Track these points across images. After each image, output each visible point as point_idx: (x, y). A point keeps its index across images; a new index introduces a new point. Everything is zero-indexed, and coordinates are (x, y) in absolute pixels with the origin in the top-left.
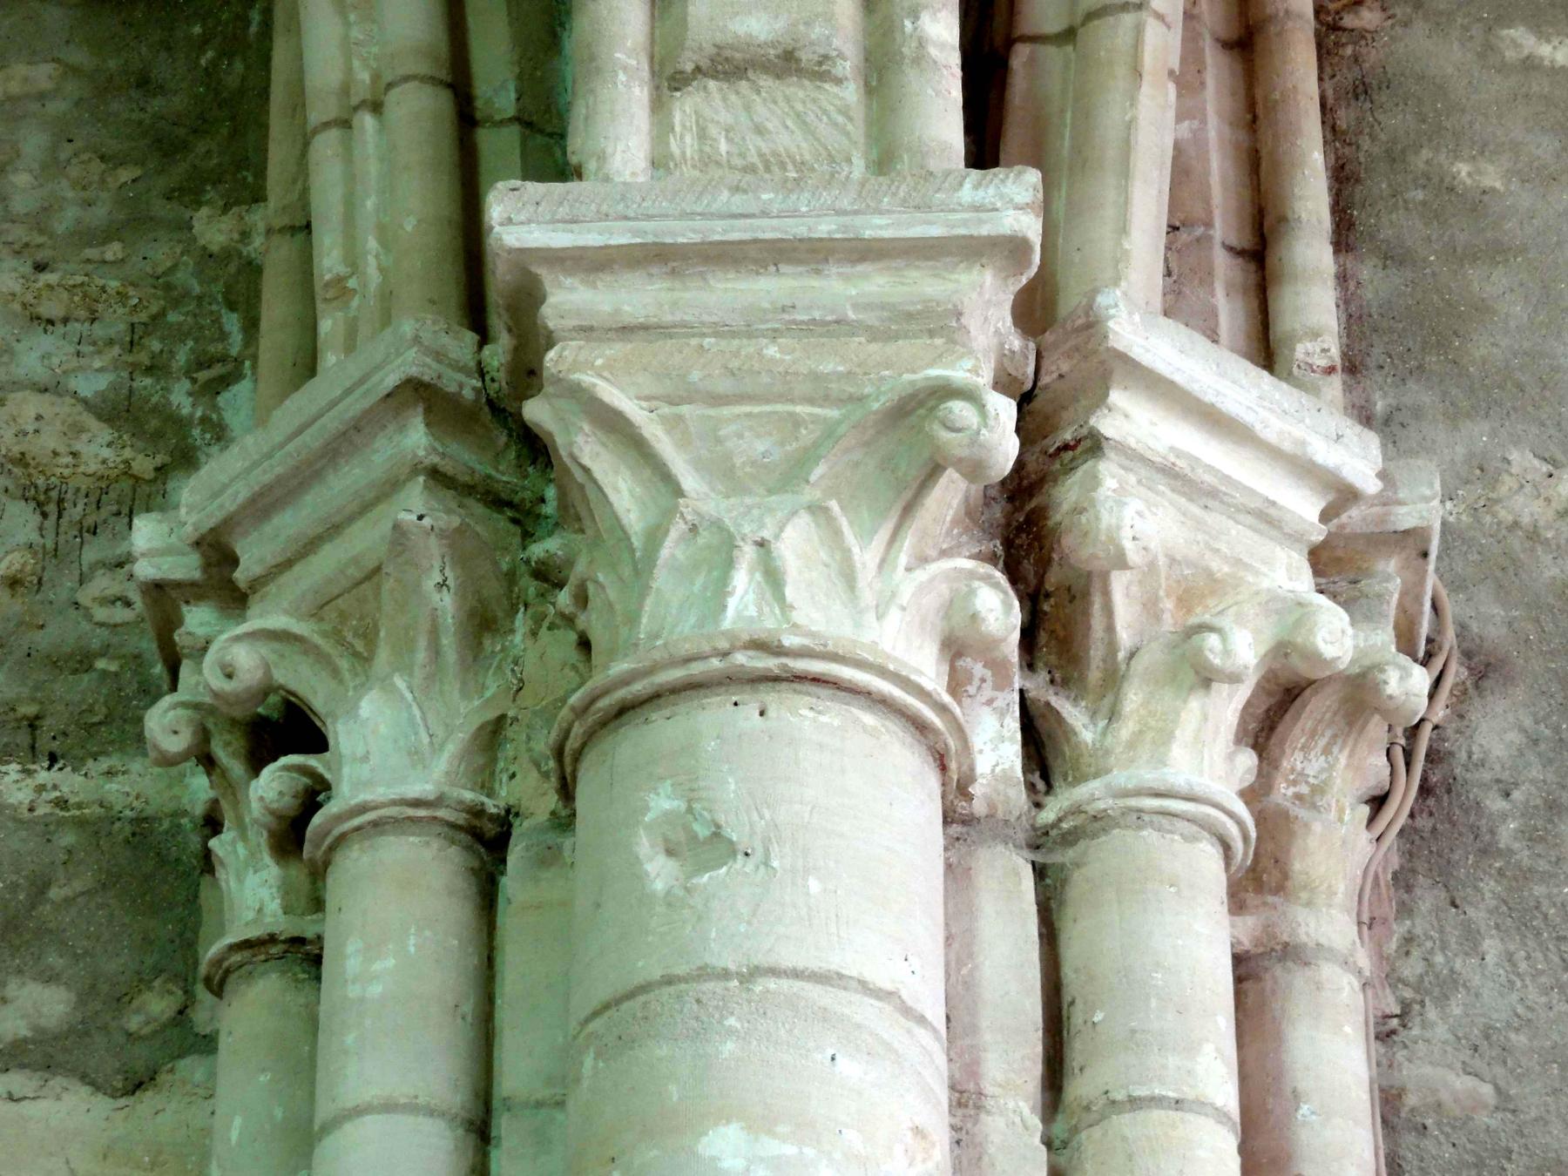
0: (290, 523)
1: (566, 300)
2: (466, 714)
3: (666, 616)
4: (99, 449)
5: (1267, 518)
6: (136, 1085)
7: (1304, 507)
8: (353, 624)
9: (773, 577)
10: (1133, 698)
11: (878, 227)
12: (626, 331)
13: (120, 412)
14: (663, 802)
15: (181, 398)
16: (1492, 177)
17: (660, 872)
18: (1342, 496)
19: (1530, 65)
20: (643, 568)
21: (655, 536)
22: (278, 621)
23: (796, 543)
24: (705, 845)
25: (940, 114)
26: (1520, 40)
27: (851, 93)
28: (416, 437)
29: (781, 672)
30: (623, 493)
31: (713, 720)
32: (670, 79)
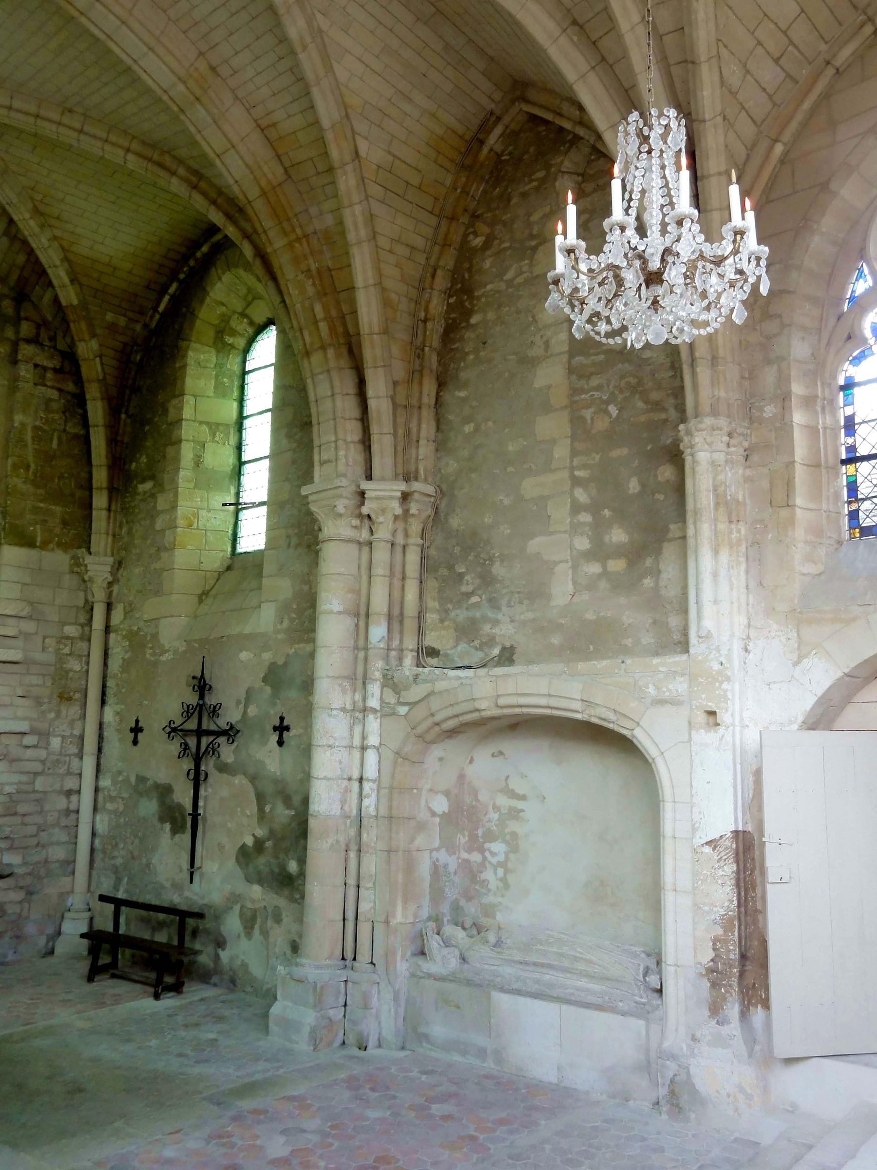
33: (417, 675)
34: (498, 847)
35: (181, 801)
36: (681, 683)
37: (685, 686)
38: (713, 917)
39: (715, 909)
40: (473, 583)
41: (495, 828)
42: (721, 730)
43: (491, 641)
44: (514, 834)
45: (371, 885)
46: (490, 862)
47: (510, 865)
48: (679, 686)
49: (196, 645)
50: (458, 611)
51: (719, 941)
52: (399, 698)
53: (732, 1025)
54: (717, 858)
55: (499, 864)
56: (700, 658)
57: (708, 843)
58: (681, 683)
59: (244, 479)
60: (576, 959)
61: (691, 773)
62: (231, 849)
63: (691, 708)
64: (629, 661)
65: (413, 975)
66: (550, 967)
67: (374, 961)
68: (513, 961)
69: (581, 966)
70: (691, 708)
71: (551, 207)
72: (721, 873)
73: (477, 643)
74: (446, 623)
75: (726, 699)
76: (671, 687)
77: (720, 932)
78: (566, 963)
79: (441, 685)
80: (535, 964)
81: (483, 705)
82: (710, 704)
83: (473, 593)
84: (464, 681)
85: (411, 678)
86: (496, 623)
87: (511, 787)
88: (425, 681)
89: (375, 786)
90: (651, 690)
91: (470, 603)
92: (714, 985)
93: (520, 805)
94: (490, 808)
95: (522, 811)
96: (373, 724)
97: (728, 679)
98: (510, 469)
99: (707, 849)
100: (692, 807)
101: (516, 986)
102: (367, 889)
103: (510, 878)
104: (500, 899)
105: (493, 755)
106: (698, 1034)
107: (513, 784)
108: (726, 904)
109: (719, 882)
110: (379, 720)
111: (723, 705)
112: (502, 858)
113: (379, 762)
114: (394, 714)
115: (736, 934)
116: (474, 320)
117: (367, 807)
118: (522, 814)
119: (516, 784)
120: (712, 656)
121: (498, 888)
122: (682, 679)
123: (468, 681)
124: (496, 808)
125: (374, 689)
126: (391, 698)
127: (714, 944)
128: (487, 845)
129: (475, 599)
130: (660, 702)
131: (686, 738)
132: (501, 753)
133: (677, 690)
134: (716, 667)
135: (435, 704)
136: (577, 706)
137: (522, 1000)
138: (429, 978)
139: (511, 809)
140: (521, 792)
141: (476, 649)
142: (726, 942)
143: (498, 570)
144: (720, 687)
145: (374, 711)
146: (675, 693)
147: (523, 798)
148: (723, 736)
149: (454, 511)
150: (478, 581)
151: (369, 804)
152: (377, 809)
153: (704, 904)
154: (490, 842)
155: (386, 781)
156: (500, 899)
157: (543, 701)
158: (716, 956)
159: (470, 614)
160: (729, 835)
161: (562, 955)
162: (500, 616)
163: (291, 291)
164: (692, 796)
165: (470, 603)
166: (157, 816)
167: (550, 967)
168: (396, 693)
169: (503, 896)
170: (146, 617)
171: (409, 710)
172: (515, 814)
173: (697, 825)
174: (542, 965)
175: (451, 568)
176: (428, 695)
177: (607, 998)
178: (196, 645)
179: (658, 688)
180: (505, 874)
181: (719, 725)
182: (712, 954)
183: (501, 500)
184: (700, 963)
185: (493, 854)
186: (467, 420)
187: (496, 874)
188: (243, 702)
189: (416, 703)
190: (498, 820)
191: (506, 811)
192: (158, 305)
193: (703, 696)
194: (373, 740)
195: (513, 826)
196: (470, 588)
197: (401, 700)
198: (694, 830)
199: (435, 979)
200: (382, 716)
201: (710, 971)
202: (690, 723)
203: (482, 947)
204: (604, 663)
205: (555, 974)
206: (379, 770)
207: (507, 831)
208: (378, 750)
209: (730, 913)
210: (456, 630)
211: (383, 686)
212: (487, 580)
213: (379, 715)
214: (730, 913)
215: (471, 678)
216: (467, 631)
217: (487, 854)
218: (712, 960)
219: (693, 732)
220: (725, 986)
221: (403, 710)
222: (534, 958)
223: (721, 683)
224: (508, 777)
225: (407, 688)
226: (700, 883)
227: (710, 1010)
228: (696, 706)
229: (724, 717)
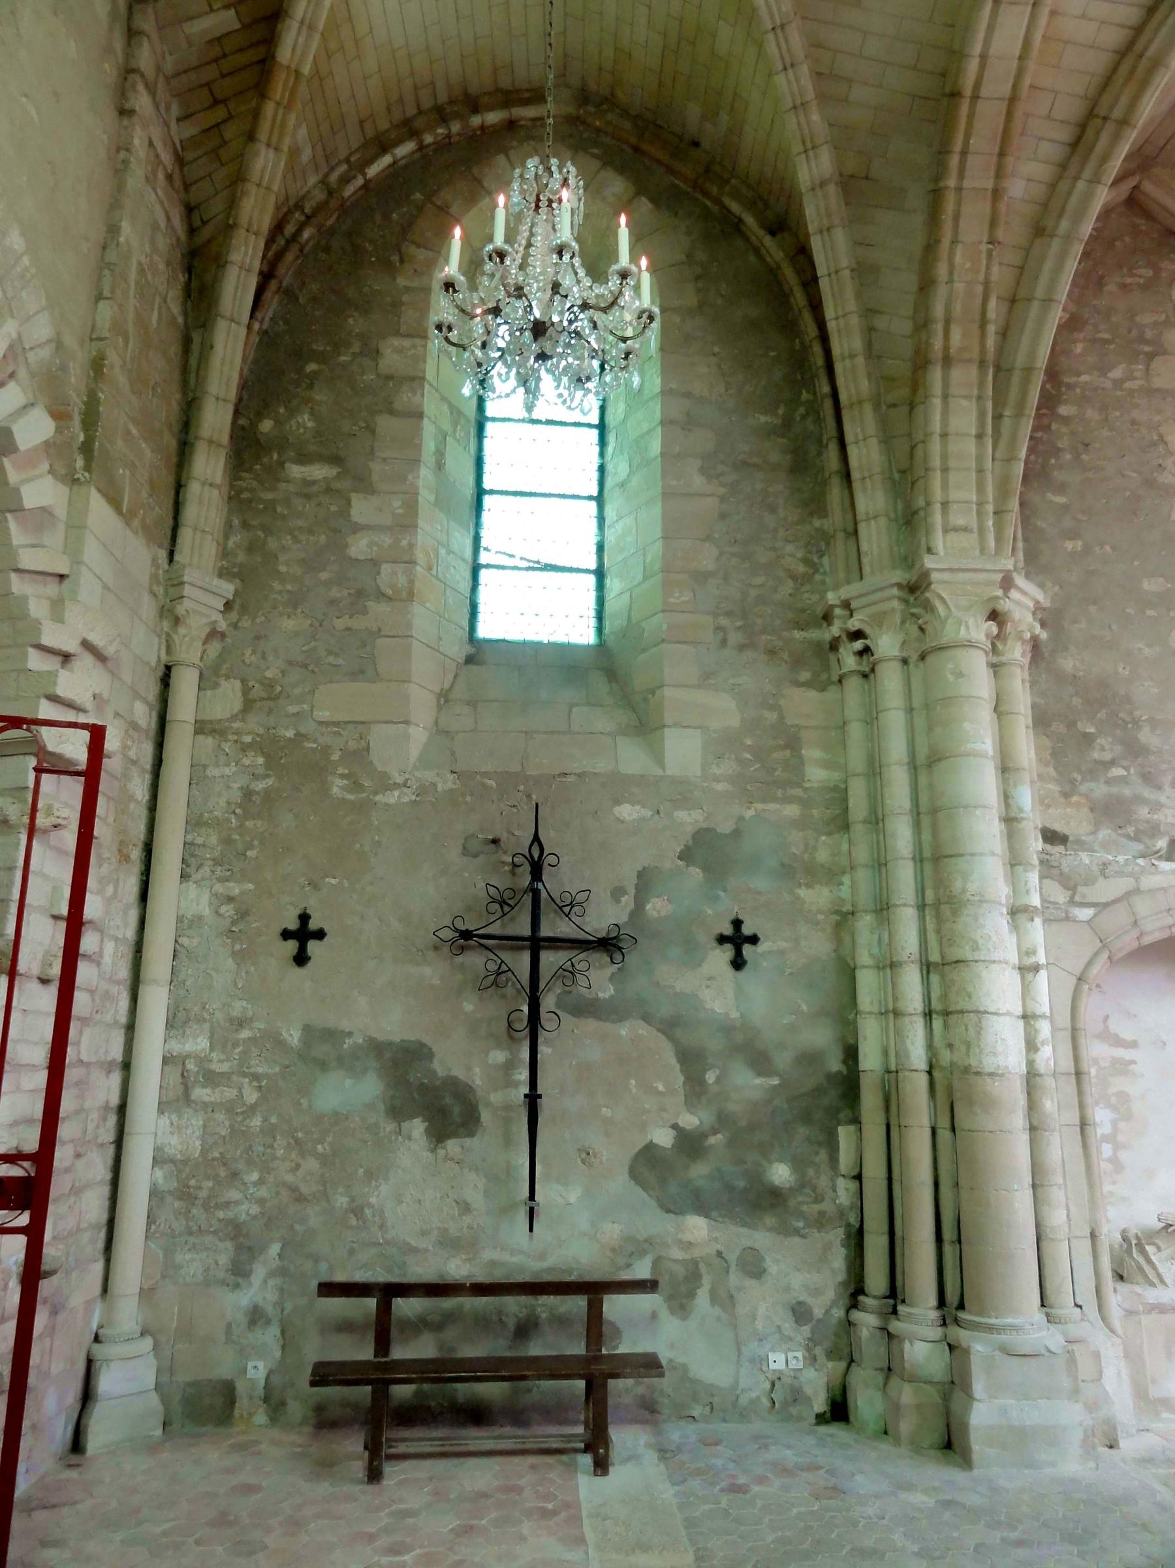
0: (864, 600)
1: (934, 576)
2: (900, 637)
3: (949, 633)
4: (802, 568)
5: (1027, 608)
6: (823, 690)
7: (1031, 605)
8: (879, 620)
9: (967, 628)
10: (1009, 643)
11: (988, 567)
12: (945, 582)
13: (806, 561)
14: (950, 666)
15: (816, 559)
16: (1044, 526)
17: (951, 678)
18: (1037, 602)
19: (1051, 501)
20: (943, 623)
21: (947, 618)
22: (861, 617)
23: (971, 622)
24: (960, 675)
25: (991, 543)
26: (1049, 495)
27: (976, 535)
28: (895, 591)
29: (970, 645)
30: (941, 609)
31: (960, 653)
32: (946, 531)
33: (1104, 864)
35: (458, 1073)
40: (1112, 750)
43: (1154, 830)
44: (1124, 1097)
47: (1121, 1138)
49: (492, 783)
50: (1092, 785)
52: (1072, 897)
59: (485, 516)
62: (615, 1155)
71: (1167, 316)
73: (1130, 830)
74: (1075, 799)
79: (1150, 881)
83: (1113, 763)
85: (1095, 868)
86: (1157, 807)
88: (1120, 874)
91: (1109, 775)
95: (1134, 1062)
96: (1037, 931)
98: (1150, 613)
103: (1123, 1156)
107: (1114, 1026)
114: (1067, 918)
116: (1063, 410)
118: (1132, 1067)
125: (1033, 878)
126: (1060, 896)
129: (1117, 772)
135: (1142, 906)
138: (1150, 1312)
139: (1115, 1061)
140: (1128, 1036)
141: (1128, 837)
143: (1145, 736)
147: (1134, 1045)
149: (1066, 649)
150: (1119, 748)
159: (1114, 790)
162: (1163, 799)
163: (958, 259)
165: (1109, 775)
166: (381, 1107)
168: (1068, 889)
169: (1114, 1183)
170: (323, 715)
171: (1095, 915)
172: (1122, 1068)
175: (1071, 725)
176: (1128, 895)
178: (492, 783)
183: (1140, 649)
186: (1074, 535)
188: (632, 891)
189: (1106, 905)
192: (369, 162)
196: (1107, 756)
207: (1111, 1090)
210: (1092, 810)
211: (1041, 878)
212: (1134, 750)
216: (1112, 812)
221: (1085, 914)
224: (1107, 1017)
225: (1089, 881)
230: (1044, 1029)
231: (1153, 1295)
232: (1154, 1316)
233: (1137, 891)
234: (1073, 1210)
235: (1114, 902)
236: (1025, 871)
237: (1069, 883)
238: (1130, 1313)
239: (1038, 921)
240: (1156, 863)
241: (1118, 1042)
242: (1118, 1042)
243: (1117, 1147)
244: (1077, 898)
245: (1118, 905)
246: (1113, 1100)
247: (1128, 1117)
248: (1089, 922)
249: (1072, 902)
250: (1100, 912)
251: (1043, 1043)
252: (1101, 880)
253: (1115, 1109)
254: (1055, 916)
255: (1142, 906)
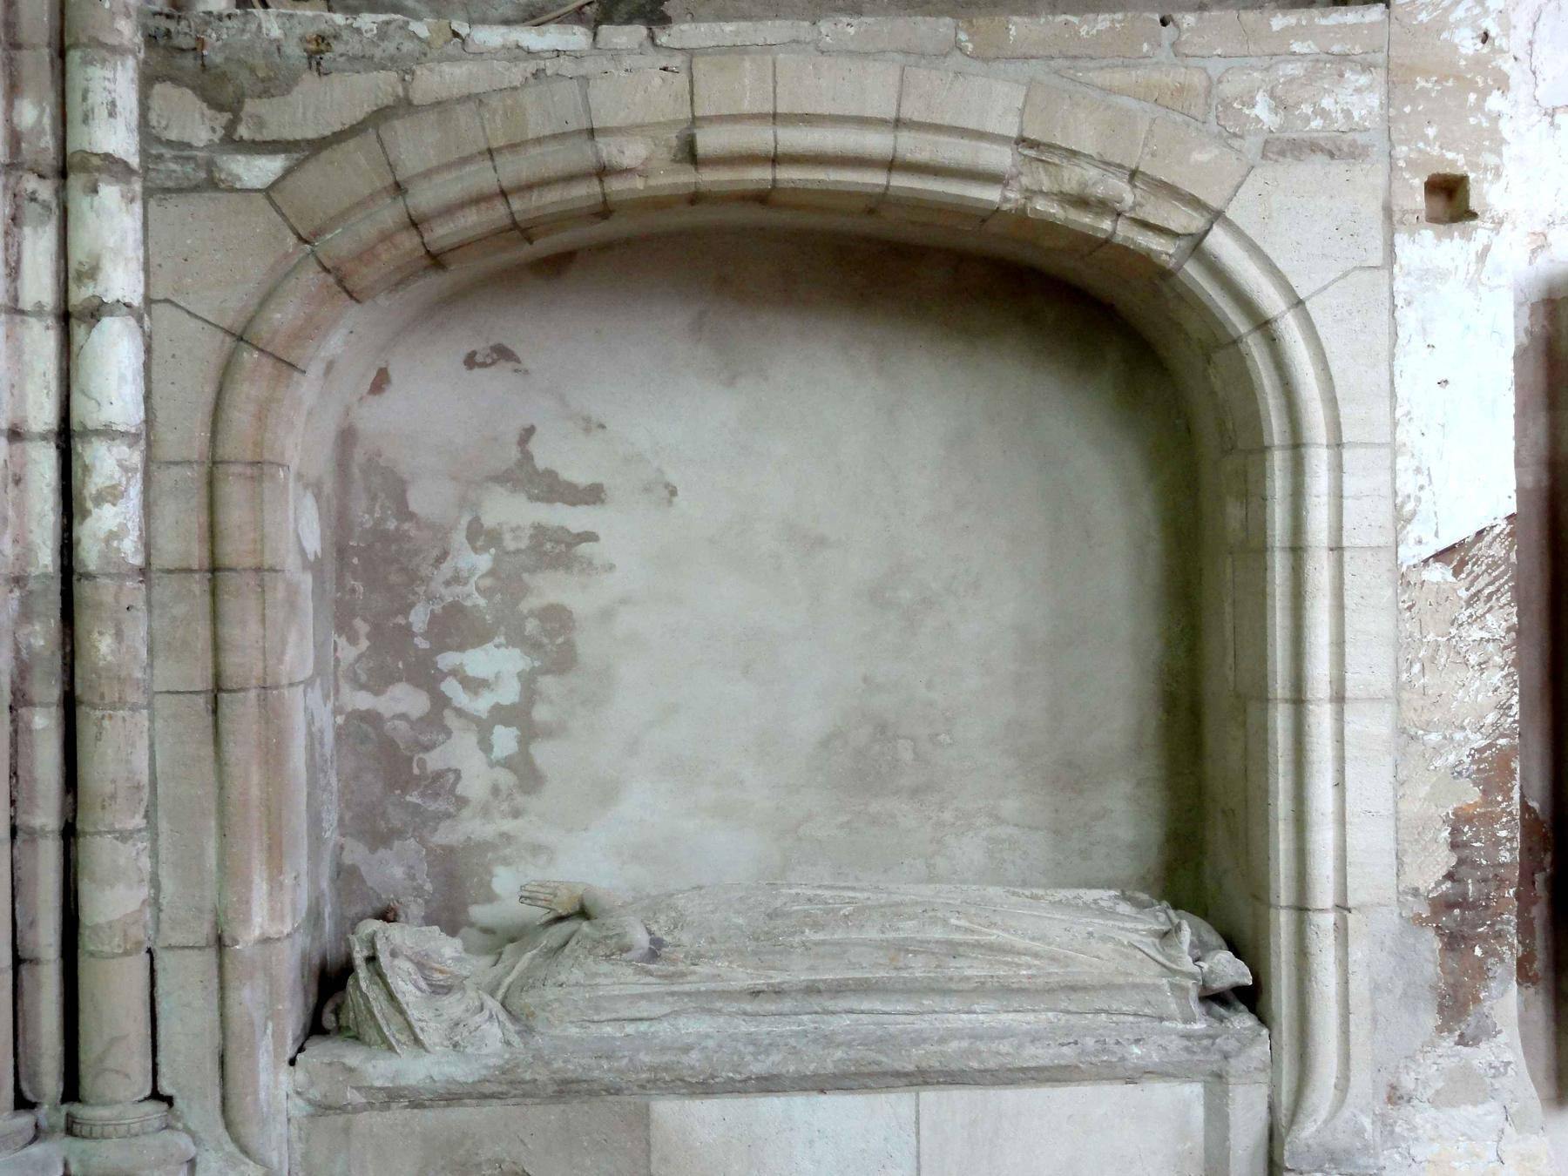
33: (321, 38)
34: (496, 665)
36: (1358, 90)
37: (1374, 100)
38: (1452, 759)
39: (1458, 736)
41: (482, 602)
42: (1481, 232)
44: (557, 618)
45: (138, 821)
46: (460, 712)
47: (541, 713)
48: (1355, 100)
51: (1469, 820)
52: (231, 127)
53: (1502, 1038)
54: (1464, 594)
55: (501, 715)
56: (1423, 17)
57: (1441, 556)
58: (1358, 90)
60: (954, 950)
61: (1392, 356)
63: (1392, 167)
64: (1188, 19)
65: (323, 1109)
66: (865, 988)
67: (165, 1087)
68: (727, 995)
69: (973, 969)
70: (1392, 167)
72: (1476, 634)
75: (1498, 142)
76: (1327, 103)
77: (1473, 795)
78: (919, 968)
79: (434, 81)
80: (812, 990)
81: (631, 152)
82: (1450, 155)
84: (550, 67)
85: (294, 51)
87: (541, 462)
89: (136, 458)
90: (1262, 110)
92: (1454, 941)
93: (575, 519)
94: (459, 538)
95: (591, 537)
96: (113, 224)
97: (1502, 83)
99: (1438, 574)
100: (1395, 455)
101: (758, 1067)
102: (124, 836)
103: (542, 753)
104: (507, 825)
105: (471, 361)
106: (1407, 1082)
107: (545, 455)
108: (1491, 718)
109: (1473, 659)
110: (137, 207)
111: (1491, 159)
112: (509, 694)
113: (147, 367)
115: (1516, 795)
117: (112, 536)
118: (584, 548)
119: (563, 454)
120: (1459, 13)
121: (495, 791)
122: (1363, 80)
123: (567, 67)
124: (479, 536)
126: (195, 124)
127: (1455, 831)
128: (447, 660)
130: (1288, 148)
131: (1377, 258)
132: (503, 353)
133: (1348, 114)
134: (1467, 43)
135: (414, 147)
136: (999, 158)
137: (772, 1106)
138: (385, 1106)
139: (541, 533)
140: (577, 474)
142: (1489, 819)
144: (1479, 106)
145: (113, 166)
146: (1341, 123)
147: (593, 495)
148: (1487, 249)
151: (112, 525)
152: (148, 545)
153: (1428, 727)
154: (461, 648)
155: (185, 435)
156: (507, 825)
157: (876, 143)
158: (1461, 862)
160: (1503, 525)
161: (902, 947)
164: (1395, 424)
167: (865, 988)
168: (219, 107)
169: (516, 814)
171: (288, 172)
172: (557, 550)
173: (1409, 507)
174: (839, 989)
176: (380, 116)
177: (1090, 1042)
179: (1281, 105)
180: (525, 741)
181: (1474, 216)
182: (1446, 858)
184: (1415, 892)
185: (474, 685)
187: (486, 745)
189: (318, 146)
190: (491, 573)
191: (524, 544)
193: (1431, 132)
194: (121, 281)
195: (550, 589)
197: (243, 131)
198: (1401, 519)
199: (416, 1104)
200: (148, 193)
201: (1443, 905)
202: (1388, 211)
203: (605, 967)
204: (1103, 21)
205: (878, 1006)
206: (147, 398)
207: (530, 604)
208: (140, 320)
209: (1502, 741)
211: (147, 81)
213: (137, 187)
214: (1502, 741)
215: (577, 57)
217: (451, 687)
218: (1449, 876)
219: (1401, 239)
220: (1482, 939)
221: (260, 170)
222: (798, 973)
223: (1484, 94)
224: (528, 433)
225: (275, 84)
226: (1417, 668)
227: (1441, 1009)
228: (1409, 162)
229: (1485, 194)
230: (106, 463)
231: (379, 1069)
232: (399, 1114)
233: (404, 106)
234: (168, 885)
235: (339, 137)
236: (87, 62)
237: (220, 90)
238: (323, 1109)
239: (110, 193)
240: (464, 30)
241: (553, 489)
242: (553, 489)
243: (530, 733)
244: (243, 131)
245: (351, 144)
246: (531, 626)
247: (563, 661)
248: (268, 191)
249: (231, 142)
250: (300, 164)
251: (100, 499)
252: (309, 80)
253: (532, 646)
254: (167, 176)
255: (414, 147)
